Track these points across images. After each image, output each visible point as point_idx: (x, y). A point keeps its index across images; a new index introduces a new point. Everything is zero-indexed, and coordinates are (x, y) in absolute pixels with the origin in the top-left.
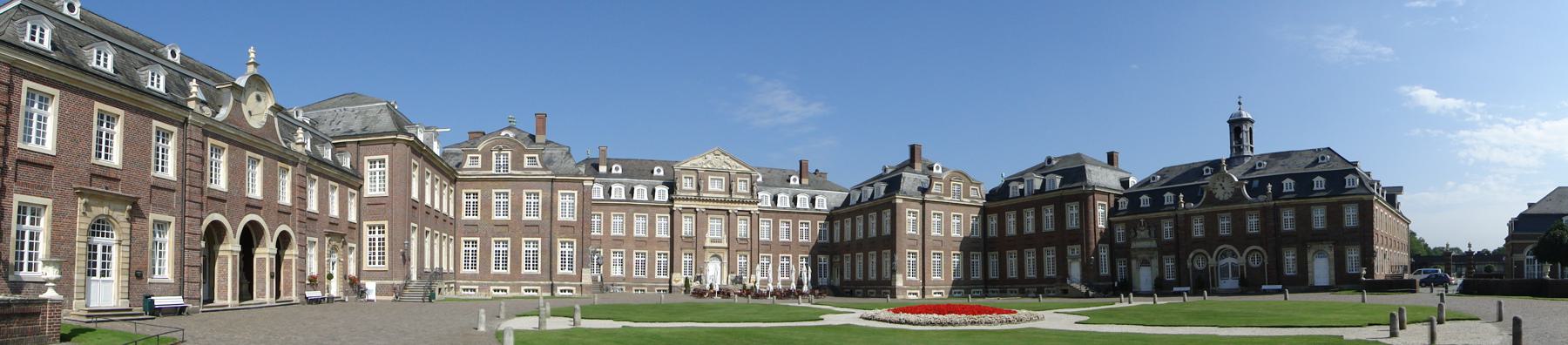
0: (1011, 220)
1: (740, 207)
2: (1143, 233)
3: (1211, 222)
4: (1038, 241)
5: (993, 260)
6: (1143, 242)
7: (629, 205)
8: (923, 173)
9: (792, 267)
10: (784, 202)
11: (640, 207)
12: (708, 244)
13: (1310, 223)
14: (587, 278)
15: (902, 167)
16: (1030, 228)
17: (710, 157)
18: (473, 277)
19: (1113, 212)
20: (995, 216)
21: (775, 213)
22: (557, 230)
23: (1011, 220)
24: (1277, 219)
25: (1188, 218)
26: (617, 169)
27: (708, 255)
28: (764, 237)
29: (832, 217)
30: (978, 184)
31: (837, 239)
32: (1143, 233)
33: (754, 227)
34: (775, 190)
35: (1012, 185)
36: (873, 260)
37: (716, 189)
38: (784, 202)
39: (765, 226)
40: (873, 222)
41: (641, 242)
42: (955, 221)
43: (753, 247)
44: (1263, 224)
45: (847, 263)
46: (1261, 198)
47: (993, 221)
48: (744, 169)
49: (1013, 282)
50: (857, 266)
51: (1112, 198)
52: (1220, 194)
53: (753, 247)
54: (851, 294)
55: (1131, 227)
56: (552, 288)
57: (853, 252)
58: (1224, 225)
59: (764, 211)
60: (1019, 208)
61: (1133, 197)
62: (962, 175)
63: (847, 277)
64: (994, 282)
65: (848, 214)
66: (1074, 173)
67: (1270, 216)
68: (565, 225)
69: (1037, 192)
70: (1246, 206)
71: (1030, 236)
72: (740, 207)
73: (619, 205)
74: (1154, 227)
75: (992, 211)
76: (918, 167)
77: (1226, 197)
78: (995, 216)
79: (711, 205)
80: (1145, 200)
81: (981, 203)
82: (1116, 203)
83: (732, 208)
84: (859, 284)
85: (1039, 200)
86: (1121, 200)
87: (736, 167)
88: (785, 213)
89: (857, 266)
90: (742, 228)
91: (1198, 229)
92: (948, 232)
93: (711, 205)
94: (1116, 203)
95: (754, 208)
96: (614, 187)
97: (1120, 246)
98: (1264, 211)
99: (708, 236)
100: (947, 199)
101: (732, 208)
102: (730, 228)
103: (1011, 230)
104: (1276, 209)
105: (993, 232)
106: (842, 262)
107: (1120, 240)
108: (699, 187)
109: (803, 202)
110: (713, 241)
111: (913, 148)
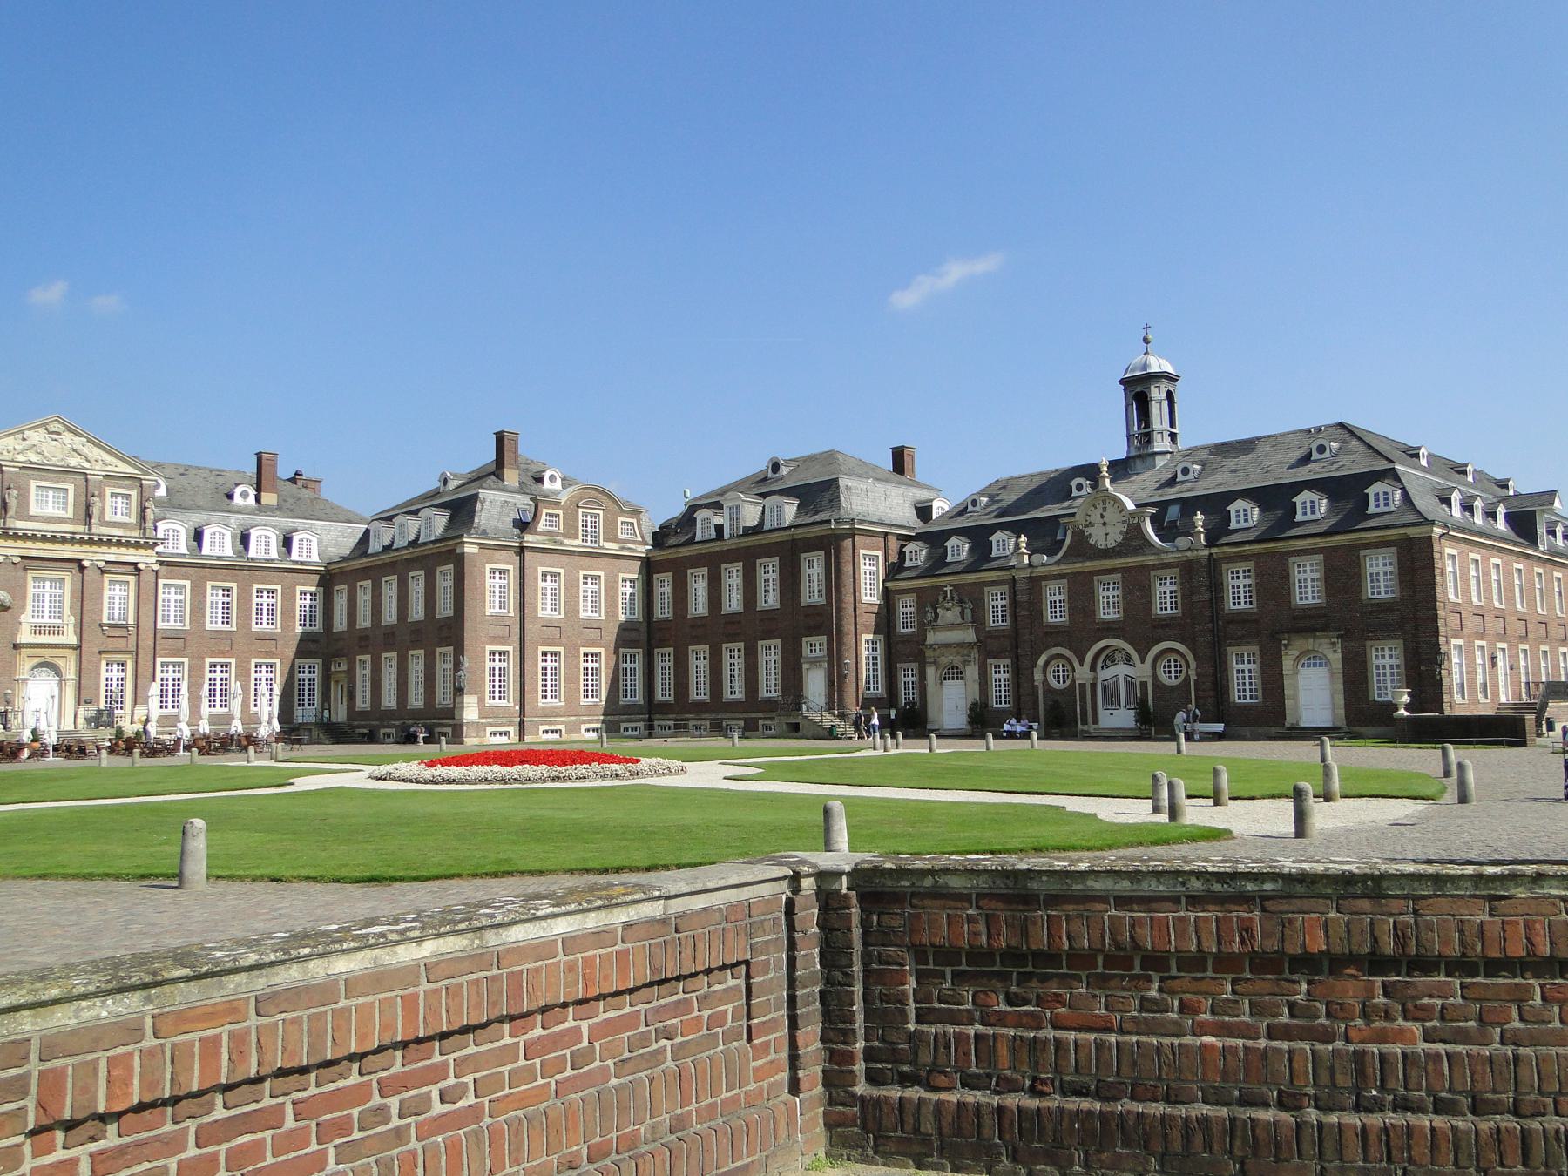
0: (699, 587)
1: (113, 554)
2: (949, 614)
3: (1081, 591)
4: (749, 627)
5: (664, 663)
6: (950, 630)
8: (522, 490)
9: (235, 687)
10: (218, 543)
12: (25, 637)
13: (1289, 592)
15: (479, 477)
16: (733, 601)
17: (36, 436)
19: (894, 570)
20: (668, 577)
21: (196, 568)
23: (699, 587)
24: (1217, 587)
25: (1036, 583)
27: (25, 664)
28: (169, 621)
29: (329, 578)
30: (636, 514)
31: (340, 623)
32: (949, 614)
33: (146, 599)
34: (197, 518)
35: (700, 515)
36: (416, 668)
37: (50, 509)
39: (173, 602)
40: (417, 589)
42: (586, 588)
43: (142, 644)
44: (1187, 595)
45: (363, 674)
46: (1182, 542)
47: (664, 587)
48: (123, 468)
49: (700, 708)
50: (385, 682)
51: (894, 544)
52: (1099, 537)
53: (142, 644)
54: (371, 738)
55: (928, 601)
57: (379, 650)
58: (1108, 603)
59: (171, 565)
60: (714, 563)
61: (936, 540)
62: (599, 495)
63: (363, 702)
64: (665, 708)
65: (365, 573)
66: (818, 494)
67: (1202, 579)
69: (749, 531)
70: (1150, 559)
71: (733, 618)
72: (113, 554)
74: (971, 599)
75: (662, 566)
76: (511, 477)
77: (1111, 543)
78: (668, 577)
79: (36, 549)
80: (959, 550)
81: (641, 550)
82: (902, 554)
83: (89, 555)
84: (388, 716)
85: (750, 549)
86: (910, 547)
87: (100, 462)
88: (219, 568)
89: (385, 682)
90: (116, 599)
91: (1055, 602)
92: (572, 609)
93: (36, 549)
94: (902, 554)
95: (145, 558)
97: (906, 640)
98: (1188, 569)
101: (89, 555)
102: (84, 601)
103: (699, 604)
104: (1213, 564)
105: (664, 609)
106: (351, 672)
107: (905, 621)
109: (264, 545)
110: (39, 630)
111: (500, 438)
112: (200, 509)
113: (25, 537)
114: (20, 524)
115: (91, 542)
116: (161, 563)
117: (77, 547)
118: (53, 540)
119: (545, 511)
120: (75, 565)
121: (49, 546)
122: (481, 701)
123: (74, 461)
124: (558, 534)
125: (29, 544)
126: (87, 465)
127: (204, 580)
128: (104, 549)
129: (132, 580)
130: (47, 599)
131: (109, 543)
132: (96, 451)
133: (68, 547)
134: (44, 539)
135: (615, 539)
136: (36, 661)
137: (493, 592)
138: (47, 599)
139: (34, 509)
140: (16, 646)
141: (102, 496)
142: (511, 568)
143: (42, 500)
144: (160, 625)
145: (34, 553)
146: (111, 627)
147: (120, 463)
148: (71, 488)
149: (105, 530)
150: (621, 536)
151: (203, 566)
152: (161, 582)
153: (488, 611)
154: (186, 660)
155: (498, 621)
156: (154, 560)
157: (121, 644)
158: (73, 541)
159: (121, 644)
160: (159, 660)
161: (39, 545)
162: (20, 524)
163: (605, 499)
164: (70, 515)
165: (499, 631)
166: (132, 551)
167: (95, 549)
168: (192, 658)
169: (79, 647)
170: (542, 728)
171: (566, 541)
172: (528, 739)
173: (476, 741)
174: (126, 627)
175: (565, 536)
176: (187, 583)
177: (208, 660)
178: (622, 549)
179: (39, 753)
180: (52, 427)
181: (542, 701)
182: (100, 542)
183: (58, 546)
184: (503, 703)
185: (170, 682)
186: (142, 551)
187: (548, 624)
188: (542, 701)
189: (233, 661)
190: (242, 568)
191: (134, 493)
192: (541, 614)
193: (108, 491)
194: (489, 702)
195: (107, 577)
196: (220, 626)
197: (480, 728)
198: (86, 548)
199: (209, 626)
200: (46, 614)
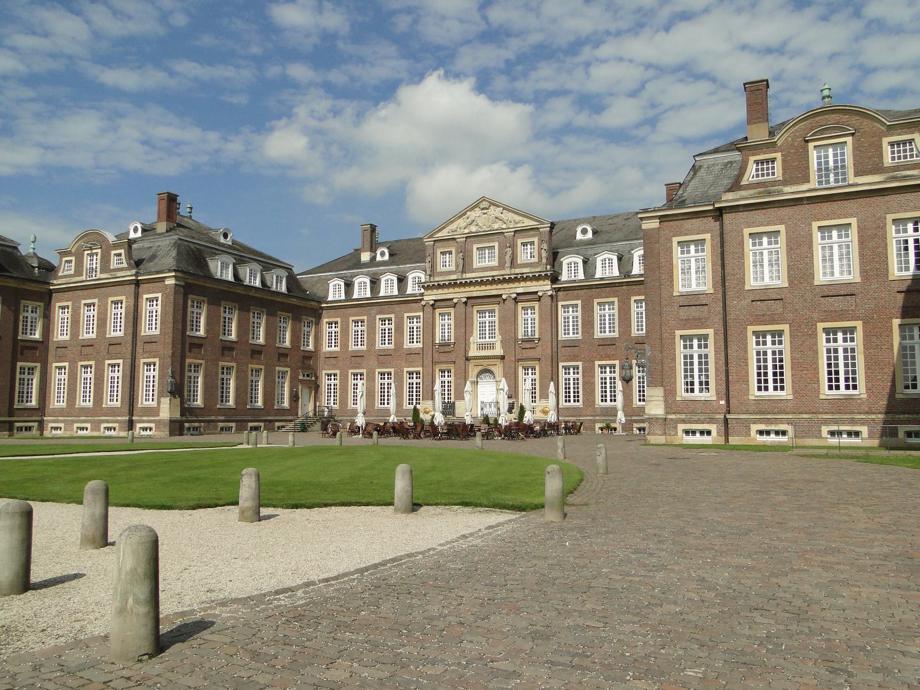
1: (521, 288)
7: (374, 304)
11: (389, 304)
12: (473, 352)
14: (167, 410)
17: (472, 215)
18: (61, 412)
21: (591, 289)
22: (139, 349)
26: (383, 254)
27: (473, 371)
28: (569, 332)
38: (606, 267)
41: (384, 357)
56: (131, 425)
68: (150, 341)
72: (521, 288)
73: (362, 305)
79: (476, 291)
88: (608, 287)
93: (476, 291)
96: (357, 281)
99: (475, 339)
100: (790, 191)
101: (509, 291)
102: (509, 323)
108: (457, 266)
110: (482, 347)
112: (608, 242)
113: (466, 284)
114: (469, 275)
115: (505, 281)
116: (559, 289)
117: (500, 286)
118: (482, 283)
119: (752, 159)
120: (499, 299)
121: (483, 287)
122: (669, 394)
123: (496, 226)
124: (774, 183)
125: (472, 288)
126: (504, 226)
127: (591, 298)
128: (517, 284)
129: (536, 305)
130: (487, 325)
131: (516, 280)
132: (510, 215)
133: (494, 287)
134: (477, 283)
135: (878, 168)
136: (480, 368)
137: (691, 271)
138: (487, 325)
139: (476, 264)
140: (467, 359)
141: (513, 247)
142: (707, 236)
143: (482, 258)
144: (562, 336)
145: (475, 294)
146: (523, 341)
147: (525, 220)
148: (496, 244)
149: (517, 271)
150: (888, 160)
151: (590, 287)
152: (560, 304)
153: (680, 288)
154: (580, 364)
155: (693, 301)
156: (549, 287)
157: (531, 354)
158: (493, 282)
159: (531, 354)
160: (561, 364)
161: (478, 288)
162: (469, 275)
163: (855, 120)
164: (495, 263)
165: (694, 312)
166: (534, 283)
167: (511, 285)
168: (584, 363)
169: (503, 358)
170: (755, 428)
171: (788, 189)
172: (734, 440)
173: (662, 440)
174: (532, 341)
175: (785, 182)
176: (579, 302)
177: (597, 363)
178: (895, 179)
179: (354, 430)
180: (482, 206)
181: (754, 393)
182: (510, 281)
183: (489, 287)
184: (704, 396)
185: (608, 381)
186: (541, 282)
187: (764, 296)
188: (754, 393)
189: (617, 362)
190: (621, 284)
191: (536, 240)
192: (751, 283)
193: (519, 242)
194: (681, 393)
195: (520, 305)
196: (608, 334)
197: (665, 424)
198: (505, 286)
199: (598, 334)
200: (487, 336)
